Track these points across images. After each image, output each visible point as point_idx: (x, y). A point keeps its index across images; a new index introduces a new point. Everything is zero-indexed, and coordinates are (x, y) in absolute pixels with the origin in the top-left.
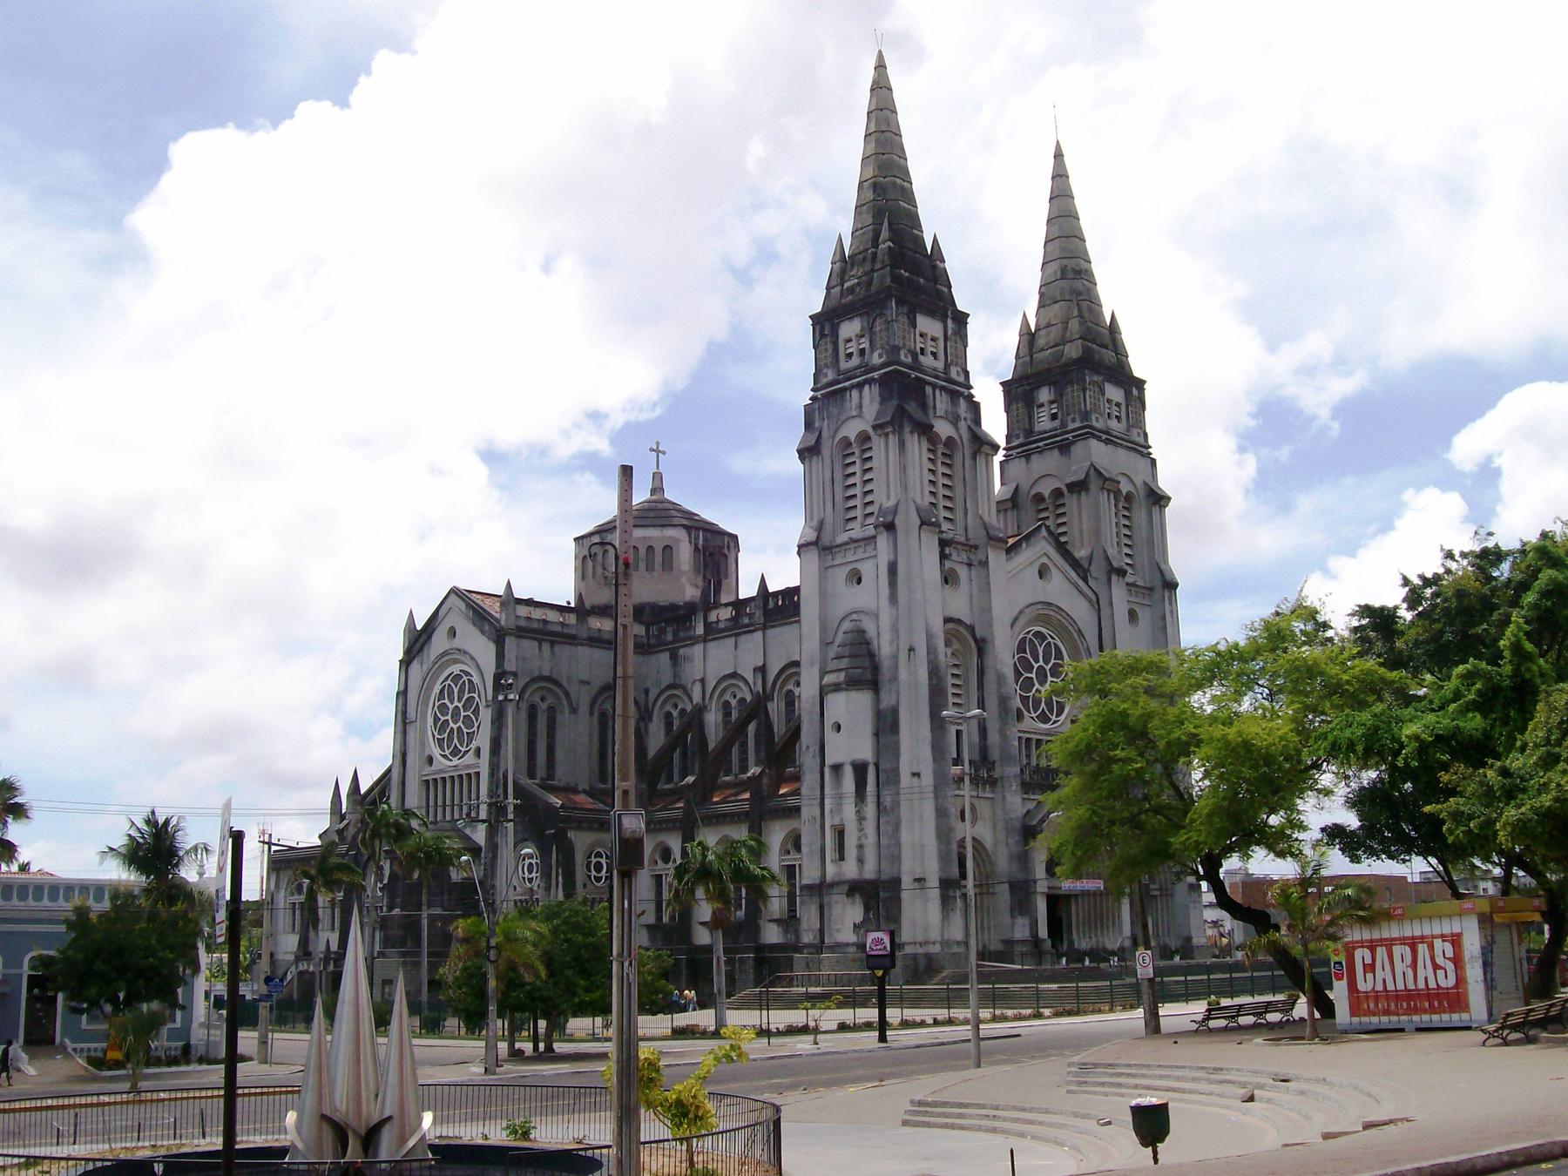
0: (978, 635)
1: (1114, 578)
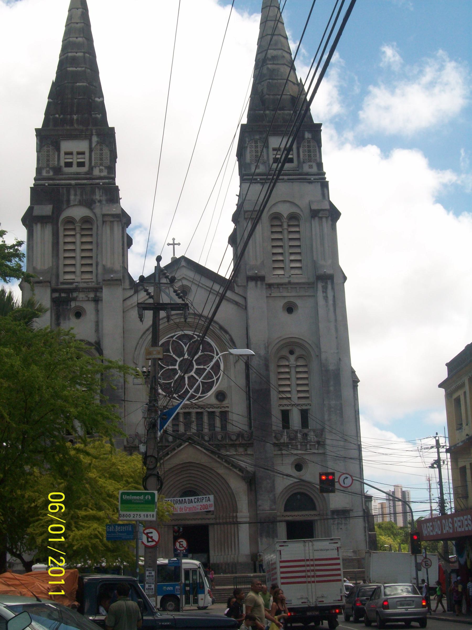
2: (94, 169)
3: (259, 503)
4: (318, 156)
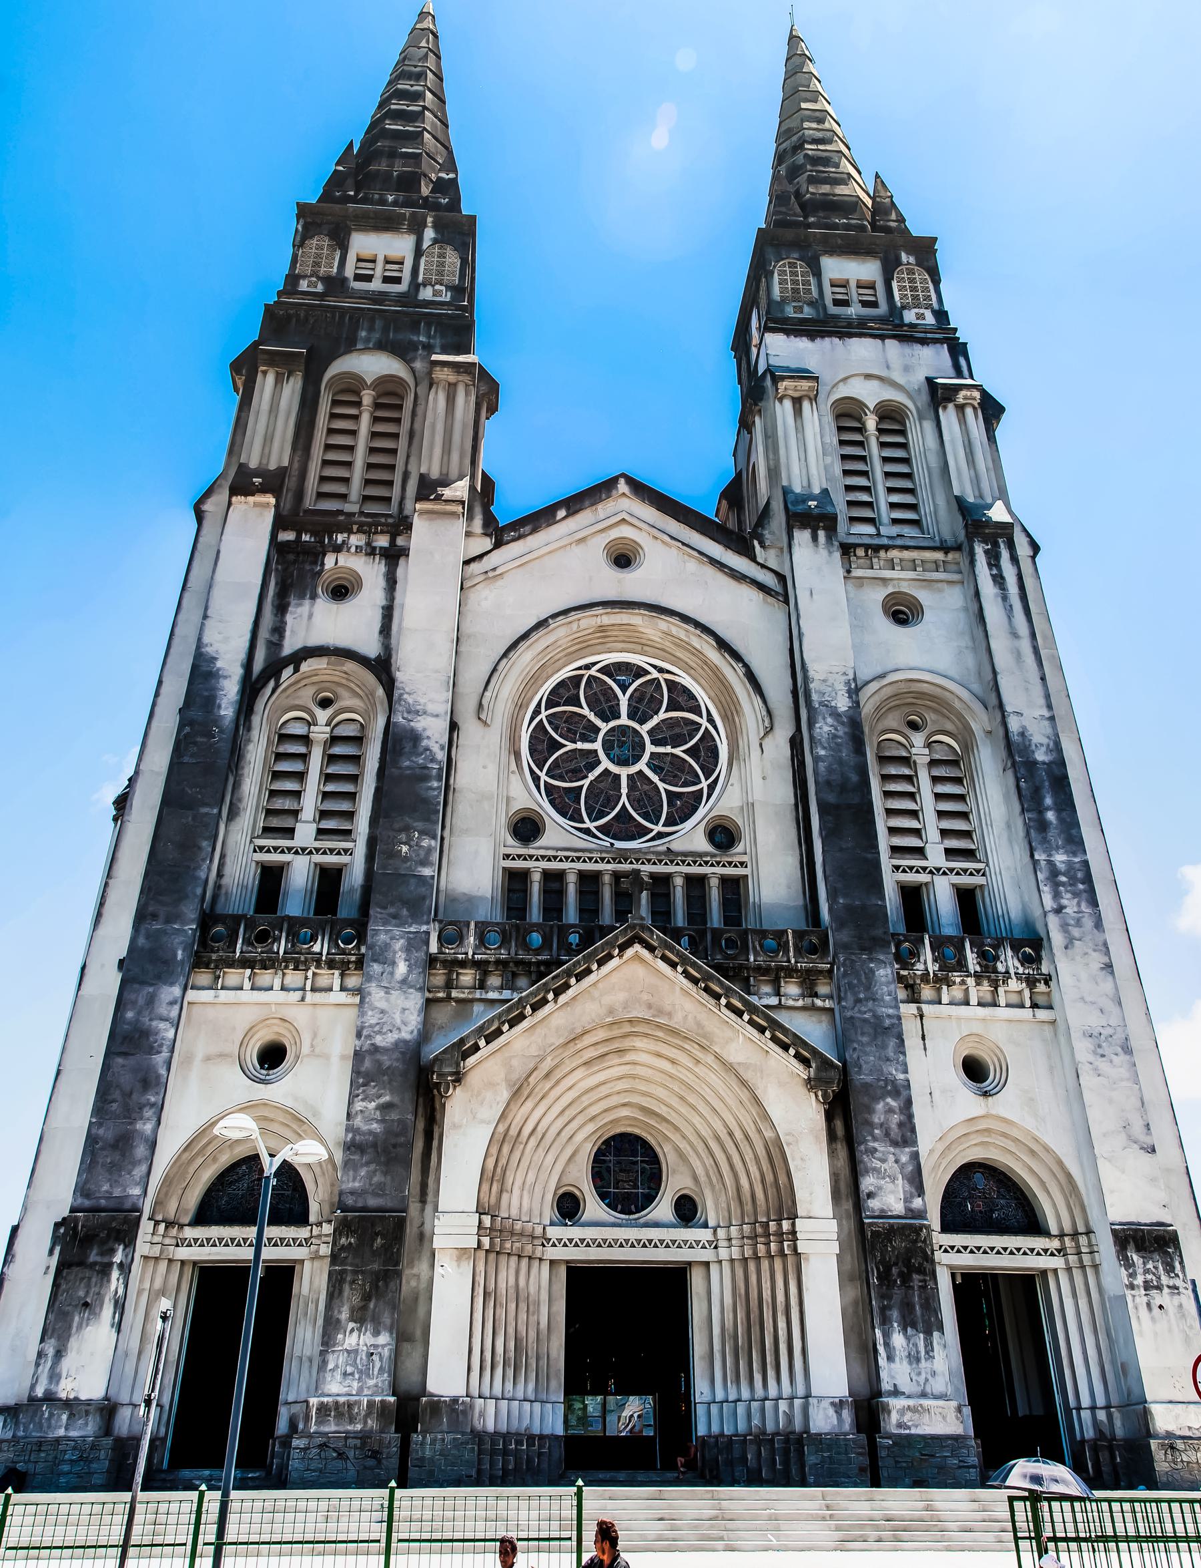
1: (802, 537)
2: (421, 288)
3: (868, 1183)
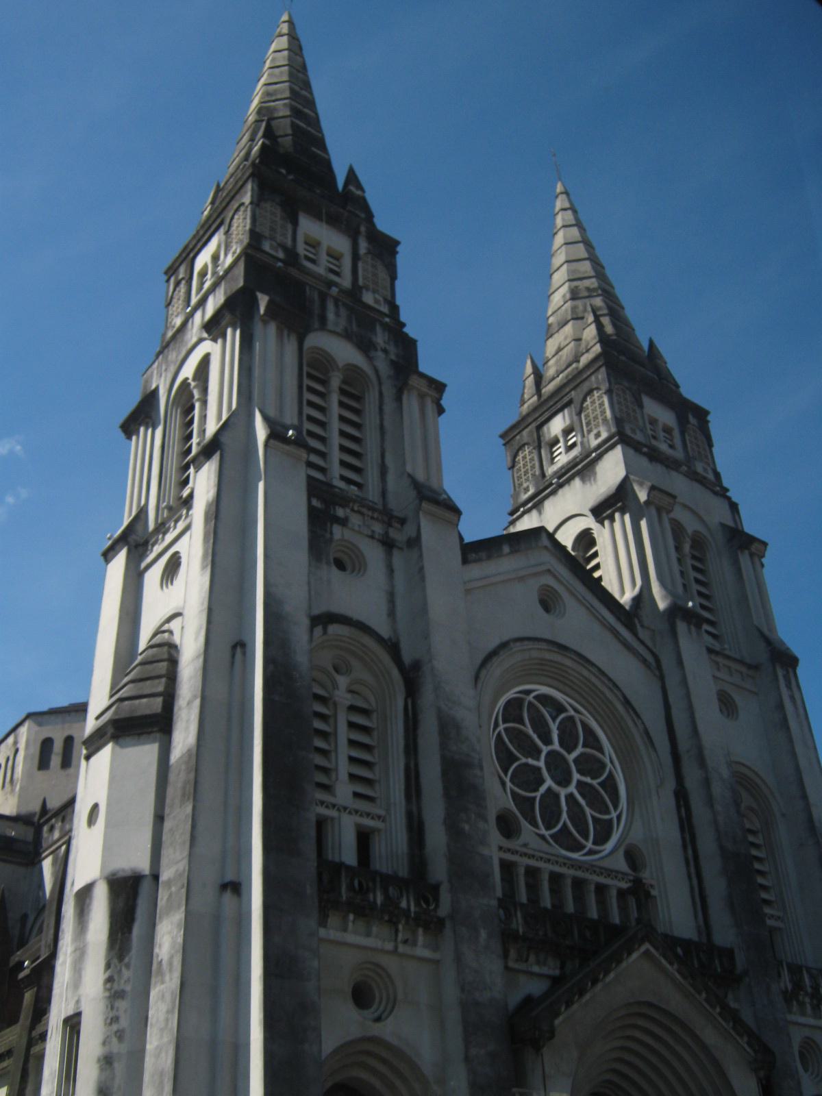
0: (407, 658)
2: (364, 291)
4: (710, 459)
